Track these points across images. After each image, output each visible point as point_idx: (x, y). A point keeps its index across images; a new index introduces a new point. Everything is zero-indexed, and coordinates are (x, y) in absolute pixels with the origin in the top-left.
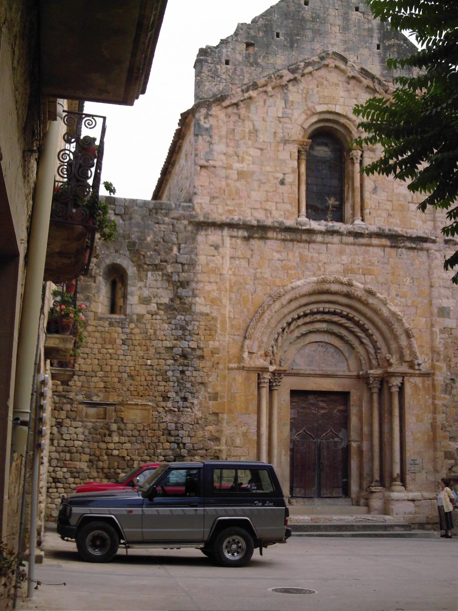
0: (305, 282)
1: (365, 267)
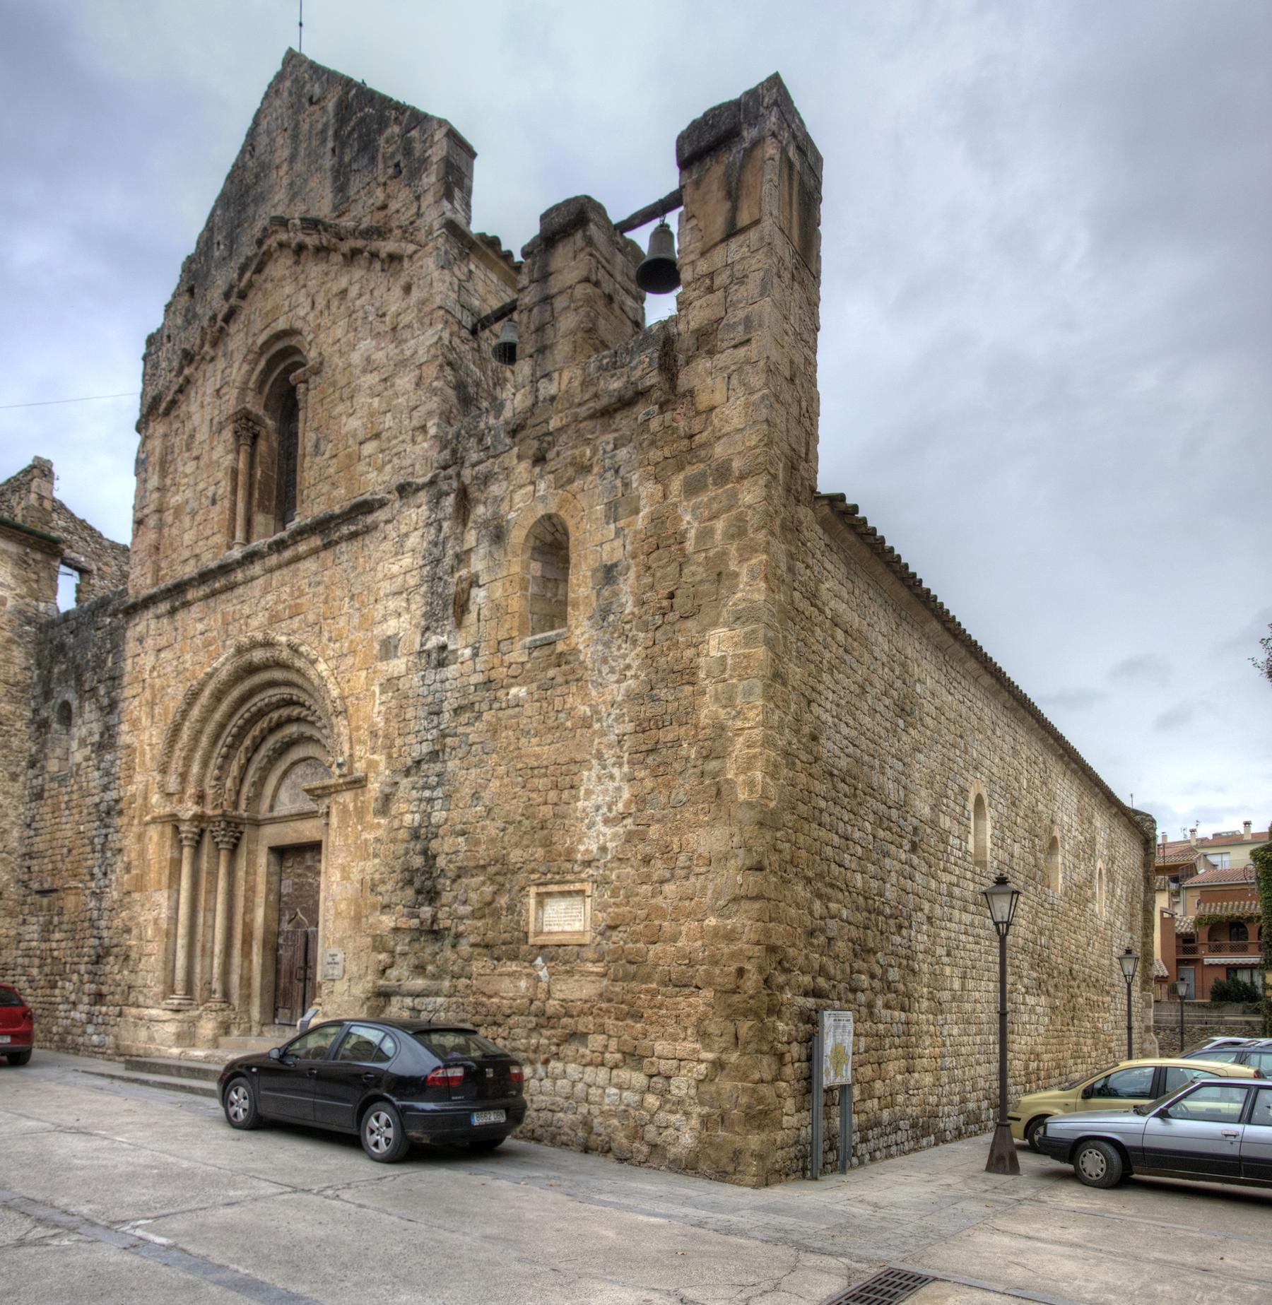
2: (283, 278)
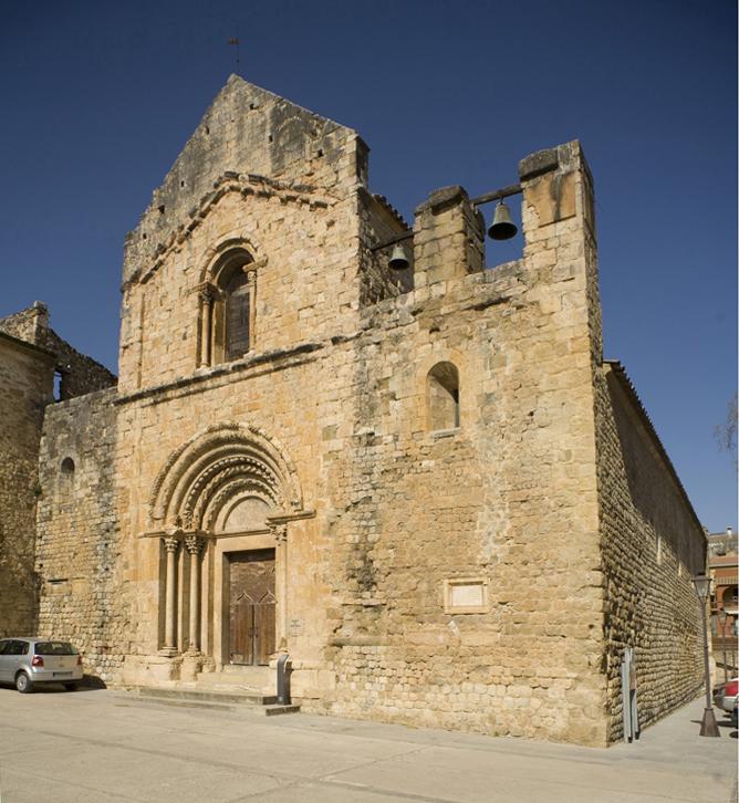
0: (198, 437)
2: (234, 208)
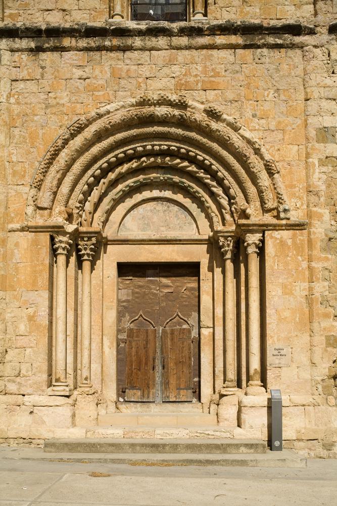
0: (119, 107)
1: (206, 79)
